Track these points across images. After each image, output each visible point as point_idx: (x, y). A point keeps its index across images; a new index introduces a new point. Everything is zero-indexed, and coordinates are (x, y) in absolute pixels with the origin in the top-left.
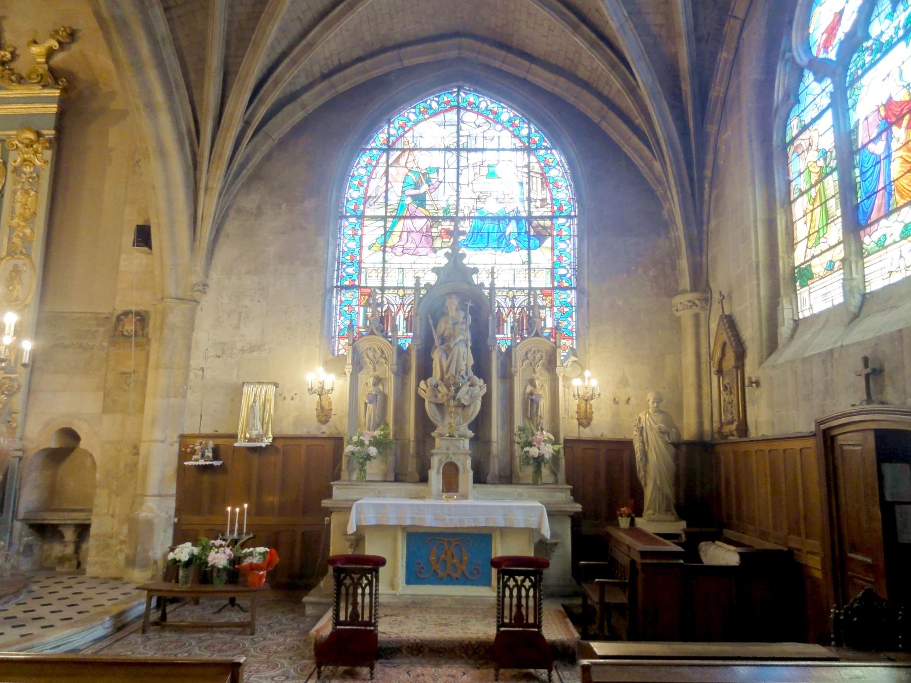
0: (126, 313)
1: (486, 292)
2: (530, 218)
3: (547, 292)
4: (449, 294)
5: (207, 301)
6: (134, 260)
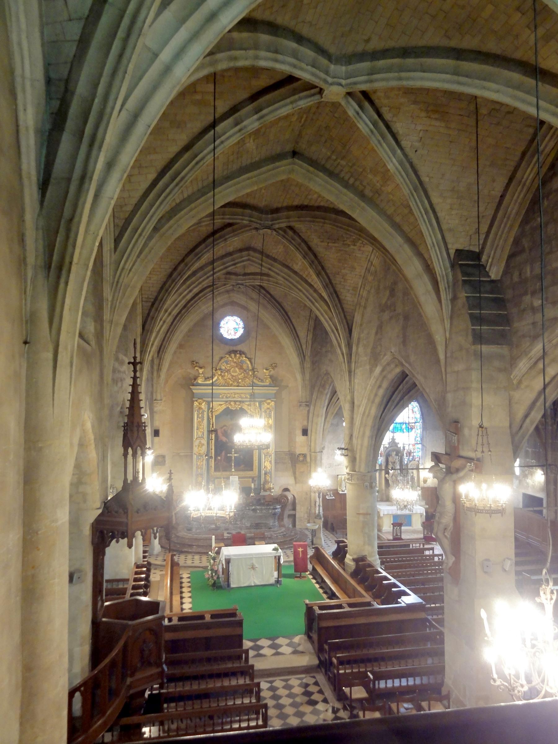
0: (300, 454)
1: (402, 448)
2: (409, 423)
3: (414, 445)
4: (393, 451)
5: (325, 451)
6: (300, 439)
